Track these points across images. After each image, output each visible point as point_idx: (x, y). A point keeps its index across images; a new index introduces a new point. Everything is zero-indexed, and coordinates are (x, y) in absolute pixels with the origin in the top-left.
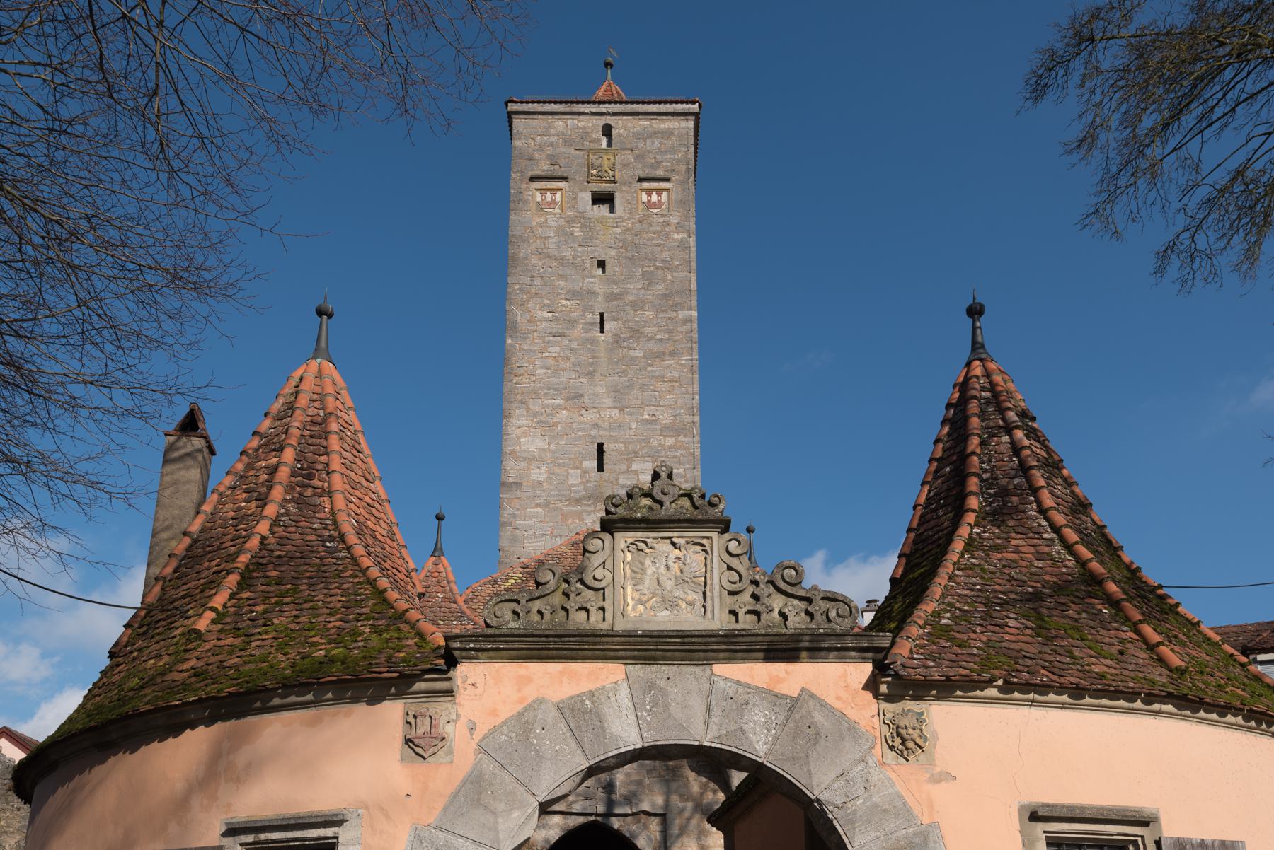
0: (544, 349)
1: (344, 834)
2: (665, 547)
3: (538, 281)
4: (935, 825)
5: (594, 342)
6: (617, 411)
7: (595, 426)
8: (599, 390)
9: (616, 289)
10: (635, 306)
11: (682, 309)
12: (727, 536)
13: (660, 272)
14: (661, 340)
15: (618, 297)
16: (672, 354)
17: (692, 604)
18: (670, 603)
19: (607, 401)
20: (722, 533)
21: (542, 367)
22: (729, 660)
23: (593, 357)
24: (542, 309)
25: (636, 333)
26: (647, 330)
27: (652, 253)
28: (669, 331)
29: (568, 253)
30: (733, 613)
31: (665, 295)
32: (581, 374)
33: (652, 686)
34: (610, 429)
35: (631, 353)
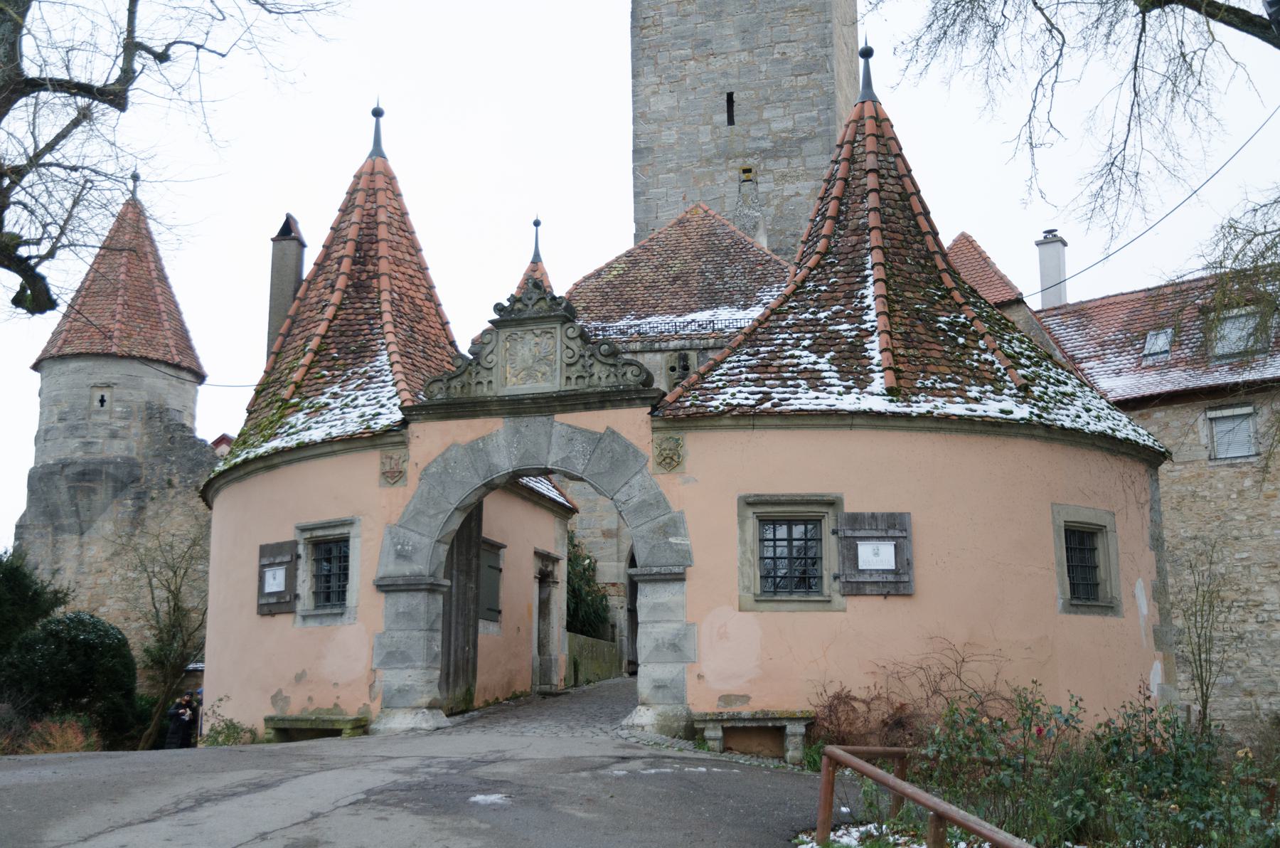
1: (353, 532)
2: (529, 336)
4: (682, 512)
12: (567, 325)
17: (544, 374)
18: (530, 374)
19: (736, 44)
20: (563, 323)
22: (563, 411)
30: (568, 378)
33: (517, 431)
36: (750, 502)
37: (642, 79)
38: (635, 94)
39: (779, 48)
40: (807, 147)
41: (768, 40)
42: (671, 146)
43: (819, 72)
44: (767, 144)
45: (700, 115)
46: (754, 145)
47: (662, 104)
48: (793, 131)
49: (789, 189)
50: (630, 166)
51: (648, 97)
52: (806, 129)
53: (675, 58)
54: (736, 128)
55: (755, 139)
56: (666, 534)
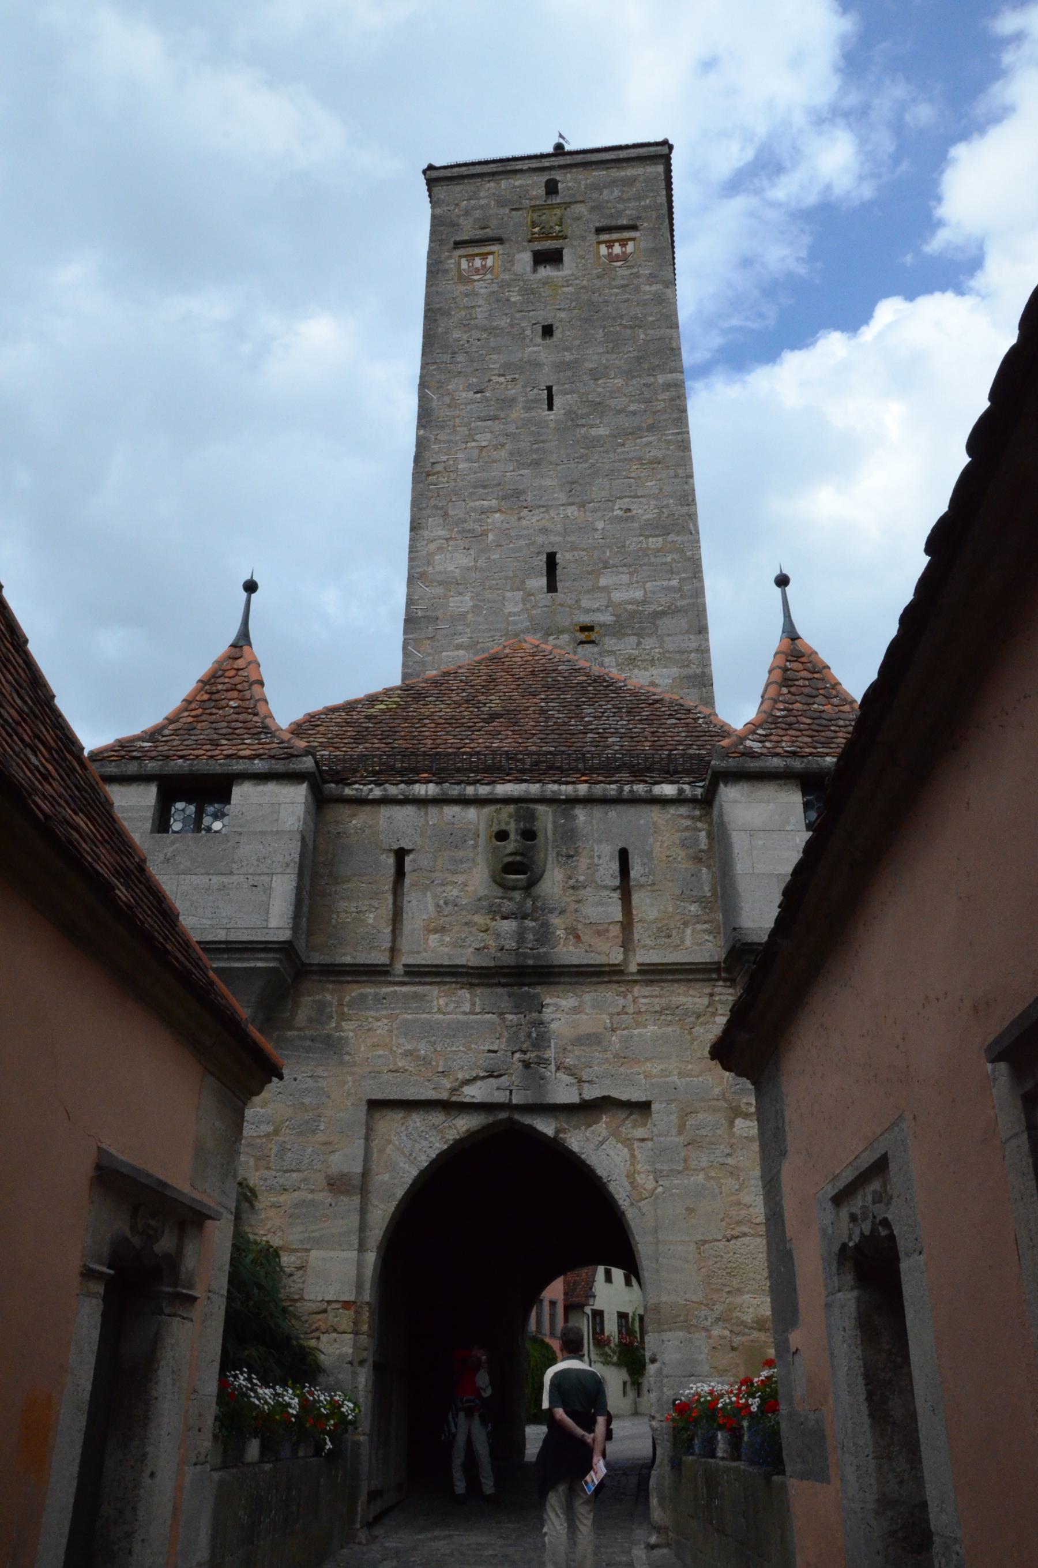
3: (461, 358)
6: (574, 507)
7: (544, 531)
8: (548, 482)
9: (568, 357)
10: (595, 375)
11: (663, 371)
14: (634, 413)
16: (651, 428)
19: (563, 498)
21: (469, 460)
23: (536, 442)
24: (469, 387)
25: (598, 407)
26: (612, 403)
31: (639, 360)
32: (522, 466)
34: (566, 532)
35: (593, 432)
37: (426, 533)
38: (412, 549)
39: (619, 504)
40: (666, 624)
41: (605, 494)
42: (463, 616)
43: (678, 533)
45: (507, 578)
47: (454, 562)
48: (644, 602)
50: (400, 638)
51: (433, 554)
53: (474, 510)
54: (559, 596)
55: (588, 611)
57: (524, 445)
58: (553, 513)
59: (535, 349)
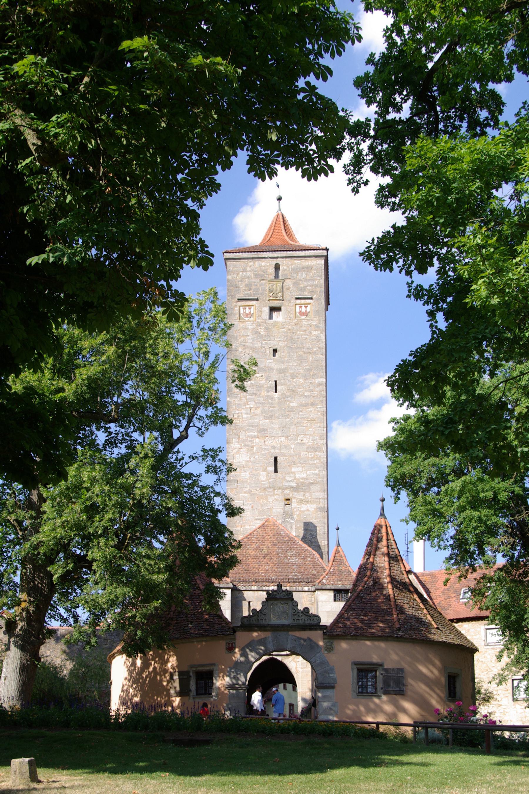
0: (247, 403)
1: (215, 668)
2: (279, 604)
5: (272, 398)
7: (274, 447)
9: (283, 366)
13: (306, 355)
14: (306, 396)
15: (283, 371)
16: (312, 404)
21: (247, 414)
25: (293, 392)
27: (302, 343)
28: (311, 391)
29: (258, 345)
31: (309, 370)
32: (265, 418)
36: (355, 663)
37: (232, 445)
40: (313, 488)
43: (319, 452)
44: (294, 484)
46: (287, 484)
48: (306, 479)
49: (304, 507)
52: (313, 479)
53: (249, 436)
55: (288, 481)
56: (329, 674)
57: (266, 409)
58: (276, 440)
59: (270, 361)
